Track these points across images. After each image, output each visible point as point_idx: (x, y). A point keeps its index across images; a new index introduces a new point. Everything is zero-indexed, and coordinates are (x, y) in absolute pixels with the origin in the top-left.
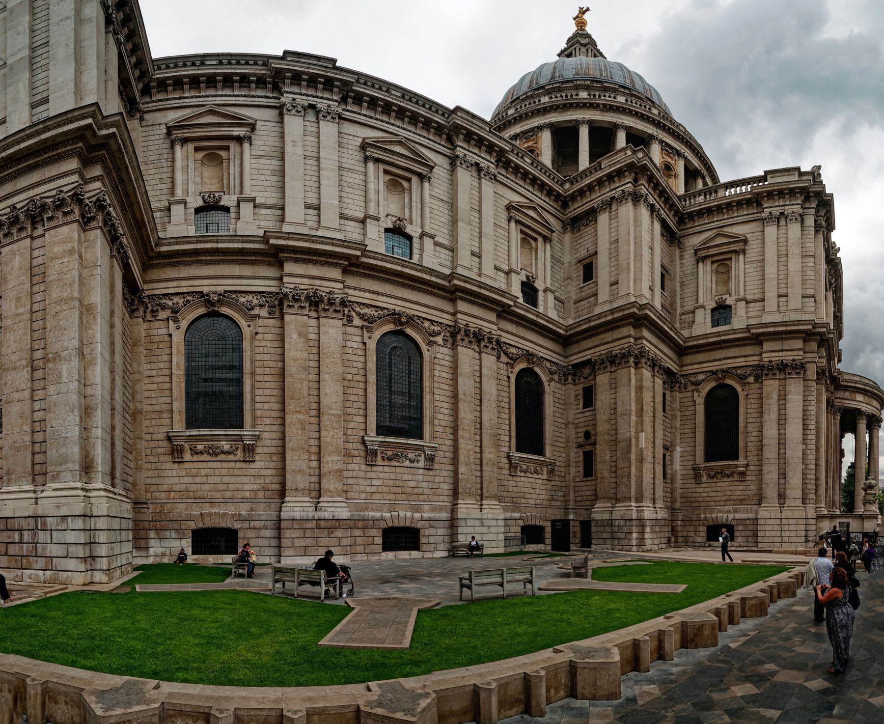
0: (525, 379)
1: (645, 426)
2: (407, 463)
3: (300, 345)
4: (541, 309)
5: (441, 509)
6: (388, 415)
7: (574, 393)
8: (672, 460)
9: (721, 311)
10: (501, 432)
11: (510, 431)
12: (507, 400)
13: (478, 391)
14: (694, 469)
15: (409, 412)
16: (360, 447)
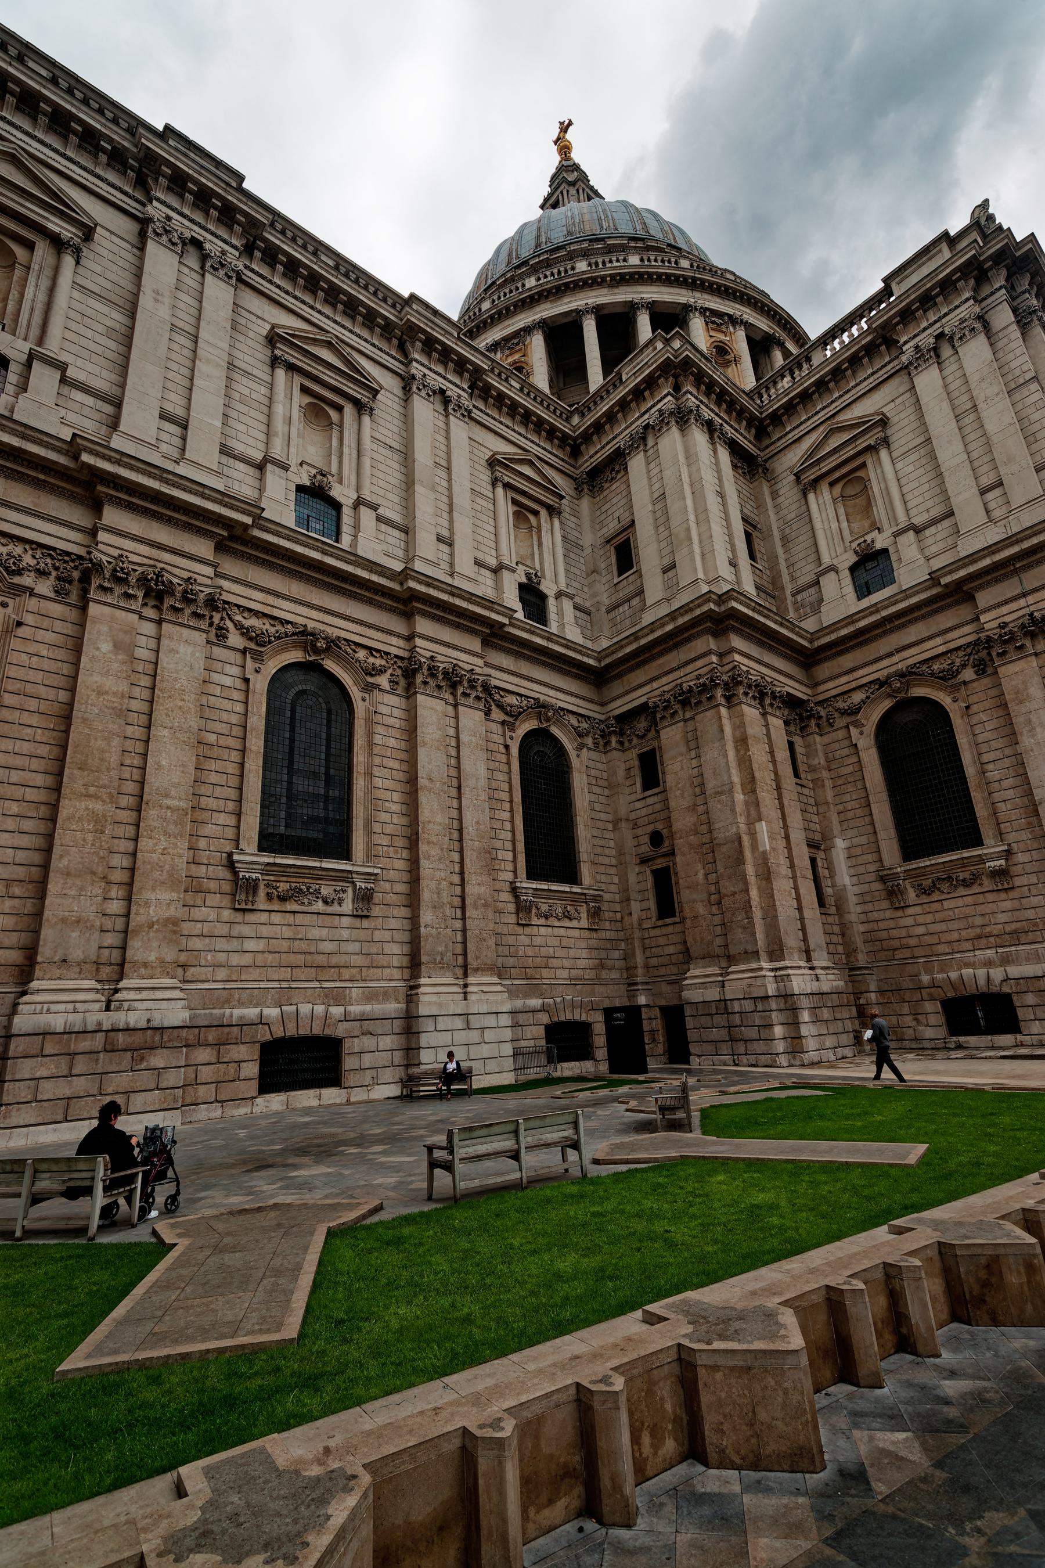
0: (536, 749)
1: (763, 810)
2: (319, 906)
3: (115, 666)
4: (554, 628)
5: (385, 995)
6: (283, 814)
7: (623, 766)
8: (830, 868)
9: (869, 565)
10: (498, 844)
11: (514, 842)
12: (505, 787)
13: (453, 772)
14: (882, 879)
15: (326, 808)
16: (224, 873)
